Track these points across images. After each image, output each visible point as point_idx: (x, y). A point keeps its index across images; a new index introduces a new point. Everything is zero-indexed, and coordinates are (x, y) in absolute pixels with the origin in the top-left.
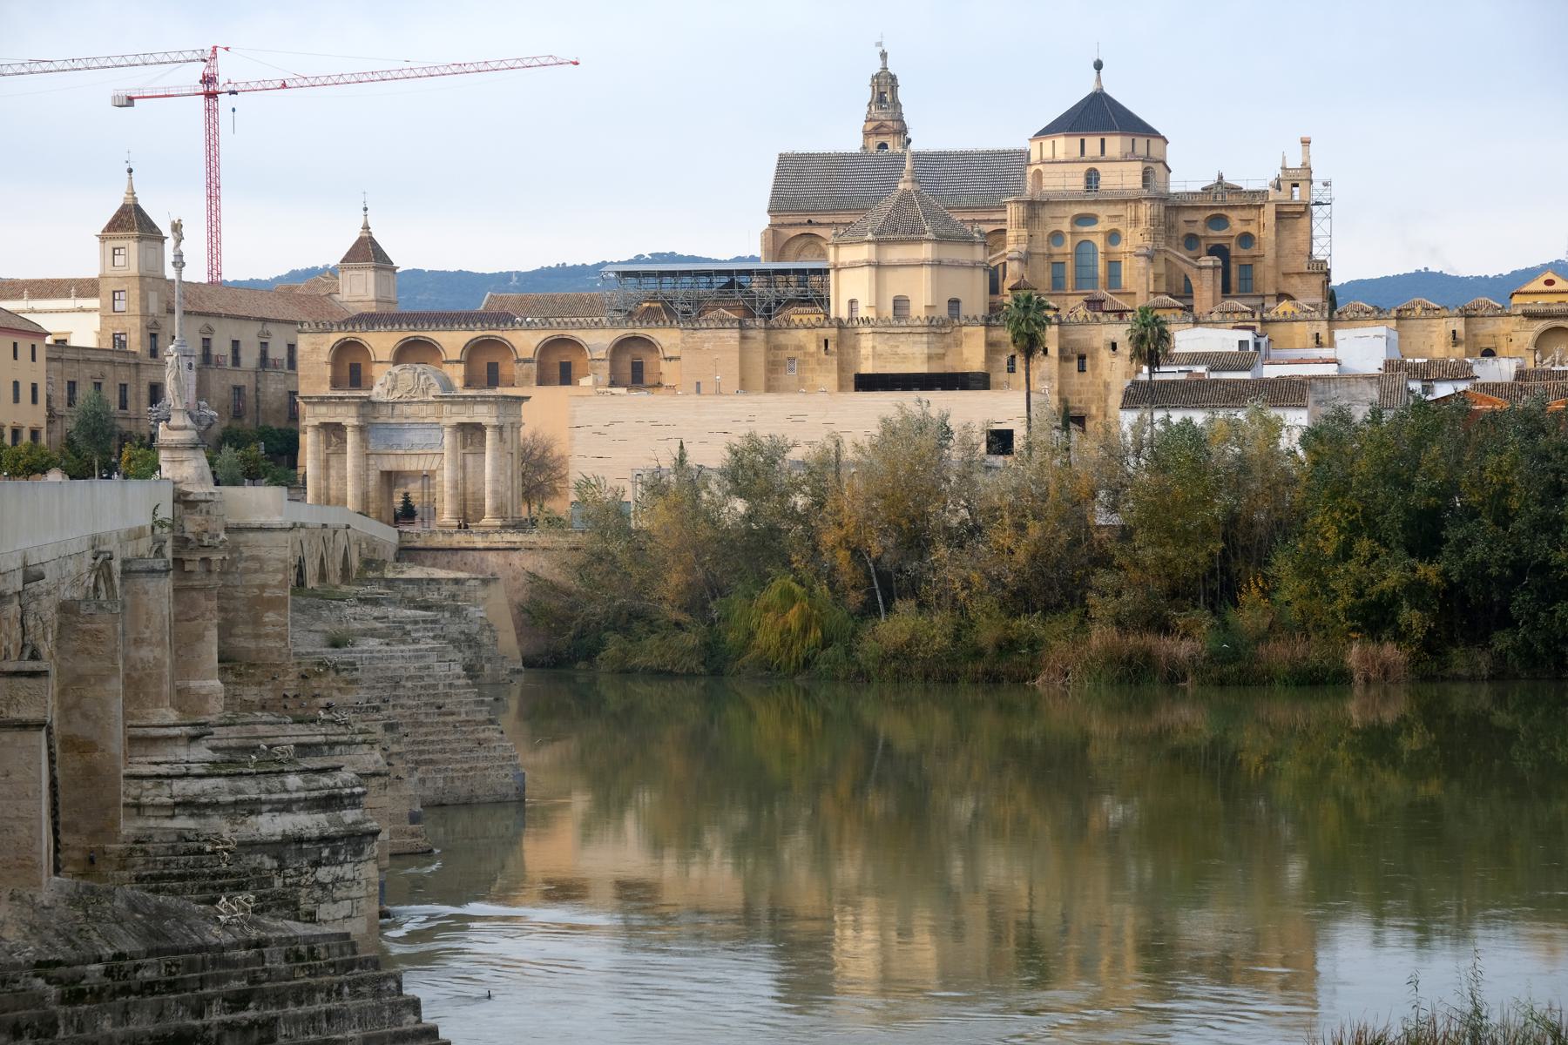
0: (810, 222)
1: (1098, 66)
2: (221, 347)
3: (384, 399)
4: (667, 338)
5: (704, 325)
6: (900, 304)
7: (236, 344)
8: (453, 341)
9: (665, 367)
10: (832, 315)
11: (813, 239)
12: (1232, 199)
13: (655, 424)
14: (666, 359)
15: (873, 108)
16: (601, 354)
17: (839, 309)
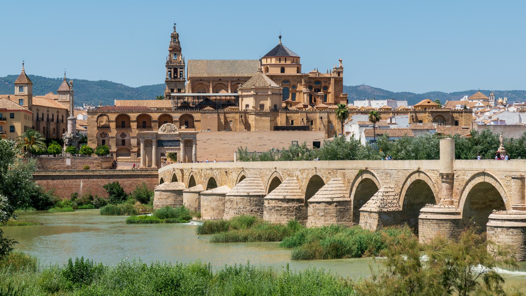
0: (201, 80)
1: (280, 37)
2: (40, 116)
3: (162, 133)
4: (197, 116)
5: (208, 111)
6: (262, 106)
7: (43, 114)
8: (133, 116)
9: (195, 123)
10: (240, 109)
11: (202, 85)
12: (320, 76)
13: (221, 140)
14: (196, 121)
15: (172, 43)
16: (177, 119)
17: (242, 106)
